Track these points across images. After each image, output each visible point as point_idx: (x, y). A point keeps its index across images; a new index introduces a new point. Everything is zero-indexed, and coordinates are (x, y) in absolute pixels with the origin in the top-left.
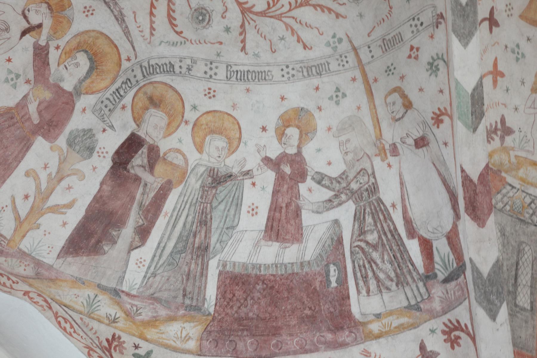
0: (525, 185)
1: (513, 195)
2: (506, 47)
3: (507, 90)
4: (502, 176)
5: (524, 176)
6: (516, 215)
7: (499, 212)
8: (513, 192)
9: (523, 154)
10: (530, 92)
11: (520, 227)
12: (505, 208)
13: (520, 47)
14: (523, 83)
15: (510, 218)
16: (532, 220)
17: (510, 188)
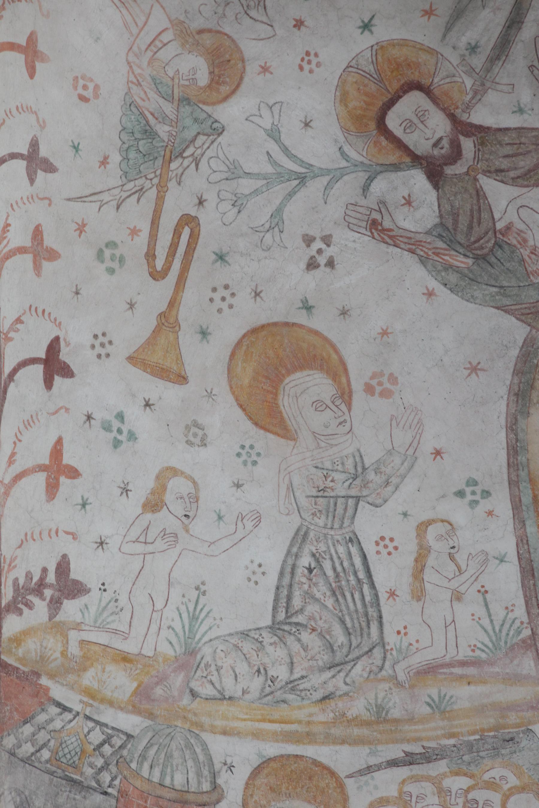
0: (95, 704)
1: (63, 727)
2: (89, 417)
3: (84, 505)
4: (41, 685)
5: (96, 685)
6: (64, 771)
7: (22, 764)
8: (62, 720)
9: (103, 638)
10: (139, 510)
11: (68, 796)
12: (38, 754)
13: (125, 419)
14: (125, 491)
15: (47, 777)
16: (98, 782)
17: (58, 710)
